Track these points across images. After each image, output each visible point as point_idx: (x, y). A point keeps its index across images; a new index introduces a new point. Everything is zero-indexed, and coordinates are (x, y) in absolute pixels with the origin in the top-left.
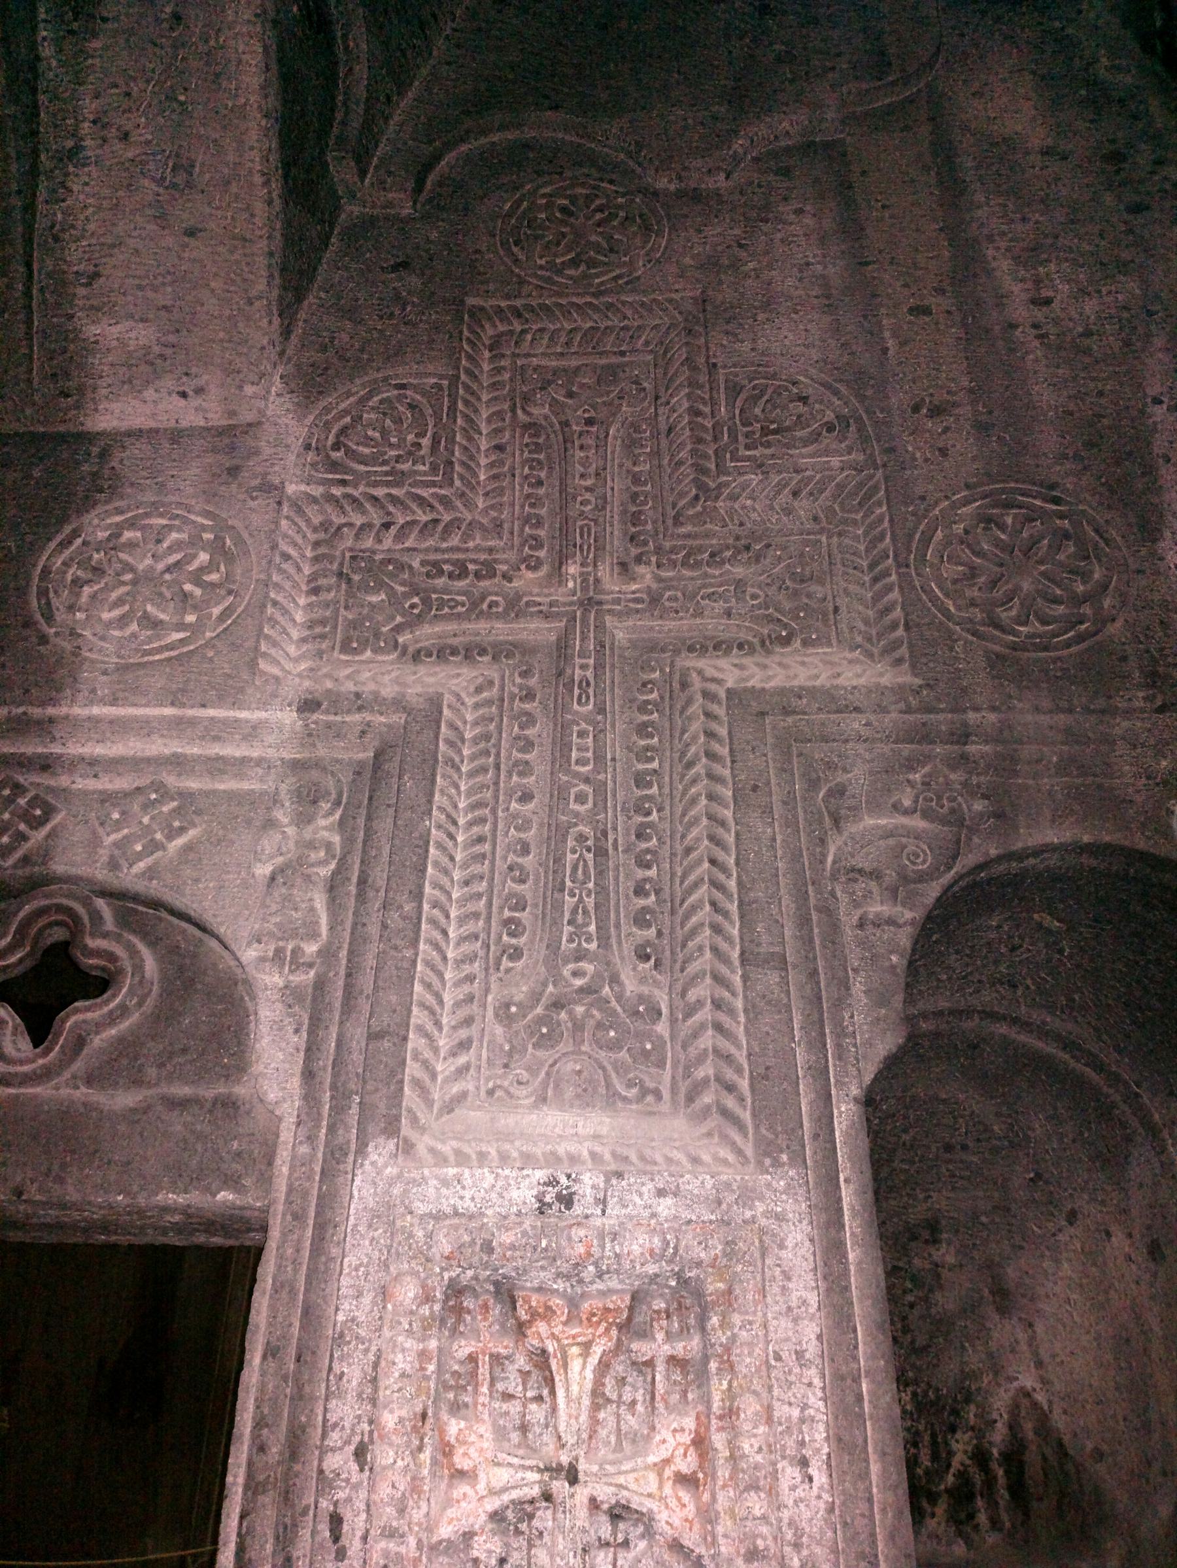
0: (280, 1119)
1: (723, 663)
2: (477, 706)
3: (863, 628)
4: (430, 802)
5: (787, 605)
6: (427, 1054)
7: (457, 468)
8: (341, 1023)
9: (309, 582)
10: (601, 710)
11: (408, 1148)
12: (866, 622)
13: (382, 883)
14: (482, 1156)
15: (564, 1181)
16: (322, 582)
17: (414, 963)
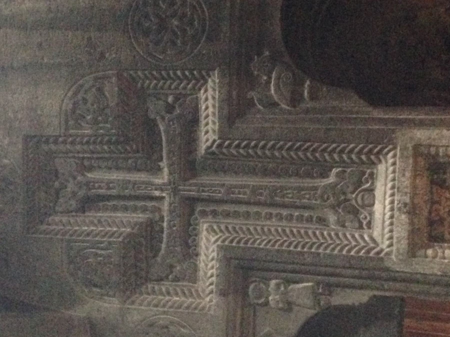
0: (375, 296)
1: (203, 138)
2: (221, 231)
3: (190, 86)
4: (263, 249)
5: (178, 111)
6: (357, 248)
7: (111, 239)
8: (345, 277)
9: (164, 296)
10: (224, 185)
11: (388, 254)
12: (188, 84)
13: (295, 266)
14: (391, 231)
15: (399, 206)
16: (164, 289)
17: (325, 254)
